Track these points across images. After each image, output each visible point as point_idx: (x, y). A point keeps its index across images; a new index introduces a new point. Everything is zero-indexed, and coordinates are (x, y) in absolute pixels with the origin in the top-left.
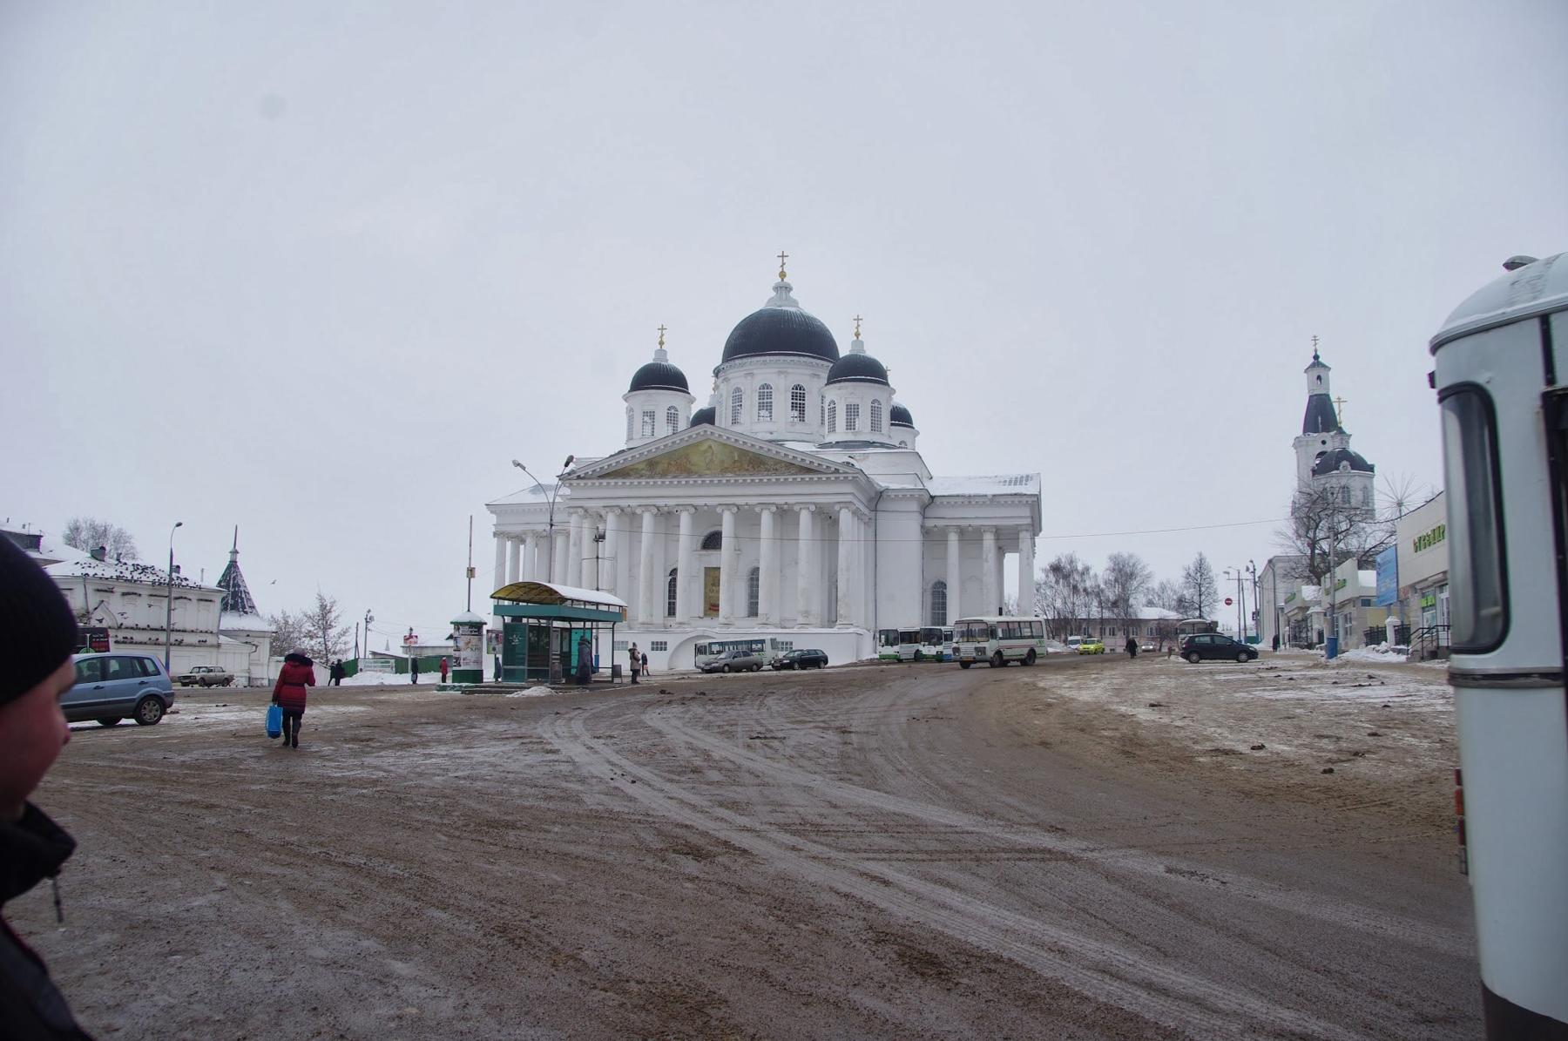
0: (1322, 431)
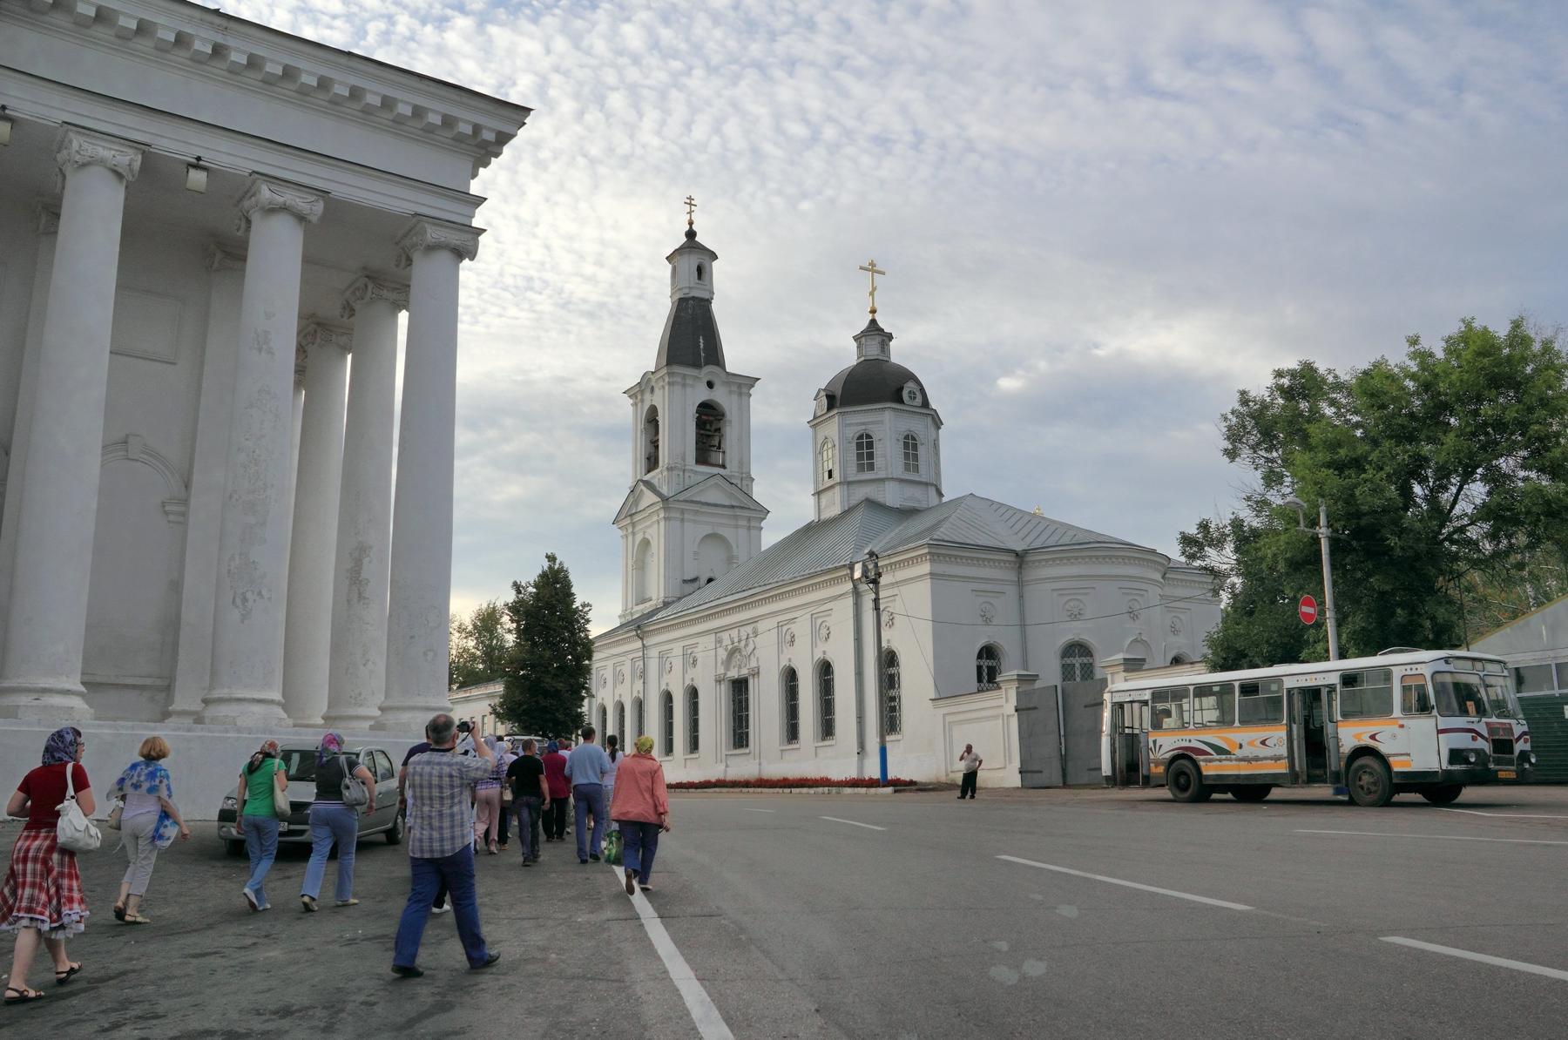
0: (707, 363)
